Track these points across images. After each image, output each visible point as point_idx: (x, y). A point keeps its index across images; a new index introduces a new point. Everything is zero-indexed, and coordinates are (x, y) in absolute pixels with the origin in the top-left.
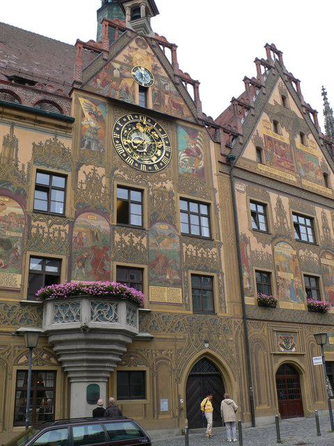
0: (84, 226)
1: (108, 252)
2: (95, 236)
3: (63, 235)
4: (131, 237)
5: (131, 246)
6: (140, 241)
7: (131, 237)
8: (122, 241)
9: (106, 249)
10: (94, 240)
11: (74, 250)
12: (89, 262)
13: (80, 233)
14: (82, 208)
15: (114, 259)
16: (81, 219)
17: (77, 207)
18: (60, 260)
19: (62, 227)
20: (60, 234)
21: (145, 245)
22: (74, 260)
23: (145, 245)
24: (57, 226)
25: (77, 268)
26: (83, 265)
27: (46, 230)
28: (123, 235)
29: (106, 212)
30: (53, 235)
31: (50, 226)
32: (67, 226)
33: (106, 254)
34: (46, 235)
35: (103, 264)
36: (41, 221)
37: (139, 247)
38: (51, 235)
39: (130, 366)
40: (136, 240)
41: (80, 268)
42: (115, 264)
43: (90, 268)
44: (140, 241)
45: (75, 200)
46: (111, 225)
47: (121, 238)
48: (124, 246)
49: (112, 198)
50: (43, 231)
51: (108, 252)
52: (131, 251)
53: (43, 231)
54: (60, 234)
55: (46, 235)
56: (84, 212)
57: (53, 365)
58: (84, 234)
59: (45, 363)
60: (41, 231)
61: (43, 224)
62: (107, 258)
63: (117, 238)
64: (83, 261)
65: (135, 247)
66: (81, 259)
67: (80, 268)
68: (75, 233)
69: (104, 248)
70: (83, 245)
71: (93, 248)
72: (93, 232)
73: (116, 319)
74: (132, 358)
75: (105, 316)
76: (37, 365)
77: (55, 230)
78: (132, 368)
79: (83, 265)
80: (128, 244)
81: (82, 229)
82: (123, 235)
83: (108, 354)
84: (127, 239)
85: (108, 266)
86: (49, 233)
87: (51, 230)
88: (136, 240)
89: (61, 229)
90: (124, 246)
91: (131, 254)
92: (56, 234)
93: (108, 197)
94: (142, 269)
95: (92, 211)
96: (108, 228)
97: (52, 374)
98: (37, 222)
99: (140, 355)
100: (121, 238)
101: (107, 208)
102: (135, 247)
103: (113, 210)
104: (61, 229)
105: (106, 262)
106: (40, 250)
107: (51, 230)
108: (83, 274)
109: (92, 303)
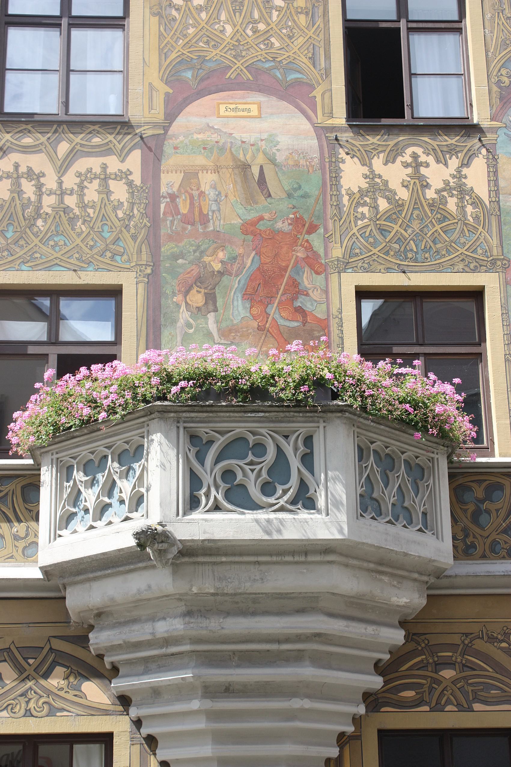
0: (205, 147)
1: (316, 241)
2: (255, 182)
3: (119, 192)
4: (416, 164)
5: (417, 202)
6: (459, 176)
7: (416, 164)
8: (376, 186)
9: (304, 225)
10: (250, 199)
11: (167, 249)
12: (235, 284)
13: (190, 176)
14: (195, 78)
15: (344, 265)
16: (200, 120)
17: (172, 77)
18: (115, 293)
19: (113, 164)
20: (106, 191)
21: (482, 191)
22: (170, 285)
23: (482, 191)
24: (94, 163)
25: (184, 315)
26: (211, 298)
27: (50, 182)
28: (378, 163)
29: (298, 83)
30: (81, 196)
31: (63, 168)
32: (136, 156)
33: (309, 248)
34: (49, 201)
35: (296, 290)
36: (26, 150)
37: (452, 204)
38: (71, 201)
39: (438, 708)
40: (437, 174)
41: (199, 312)
42: (351, 280)
43: (238, 310)
44: (459, 176)
45: (163, 53)
46: (321, 131)
47: (372, 176)
48: (383, 205)
49: (319, 22)
50: (39, 187)
51: (316, 241)
52: (421, 222)
53: (39, 187)
54: (106, 191)
55: (49, 201)
56: (200, 94)
57: (96, 711)
58: (207, 180)
59: (59, 704)
60: (28, 189)
61: (38, 162)
62: (314, 262)
63: (352, 175)
64: (209, 286)
65: (437, 206)
66: (199, 281)
67: (199, 312)
68: (170, 181)
69: (298, 222)
70: (204, 220)
71: (250, 228)
72: (245, 167)
73: (304, 499)
74: (448, 674)
75: (255, 492)
76: (28, 713)
77: (86, 177)
78: (451, 719)
79: (211, 298)
80: (403, 194)
81: (200, 160)
82: (378, 163)
83: (297, 658)
84: (395, 174)
85: (316, 295)
86: (62, 193)
87: (70, 180)
88: (437, 174)
89: (111, 169)
90: (383, 205)
91: (419, 237)
92: (92, 194)
93: (302, 20)
94: (477, 295)
95: (238, 85)
96: (311, 143)
97: (96, 749)
98: (15, 157)
99: (478, 654)
100: (372, 176)
101: (304, 61)
102: (437, 206)
103: (327, 72)
104: (111, 169)
105: (308, 280)
106: (30, 261)
107: (70, 180)
108: (209, 335)
109: (193, 438)
